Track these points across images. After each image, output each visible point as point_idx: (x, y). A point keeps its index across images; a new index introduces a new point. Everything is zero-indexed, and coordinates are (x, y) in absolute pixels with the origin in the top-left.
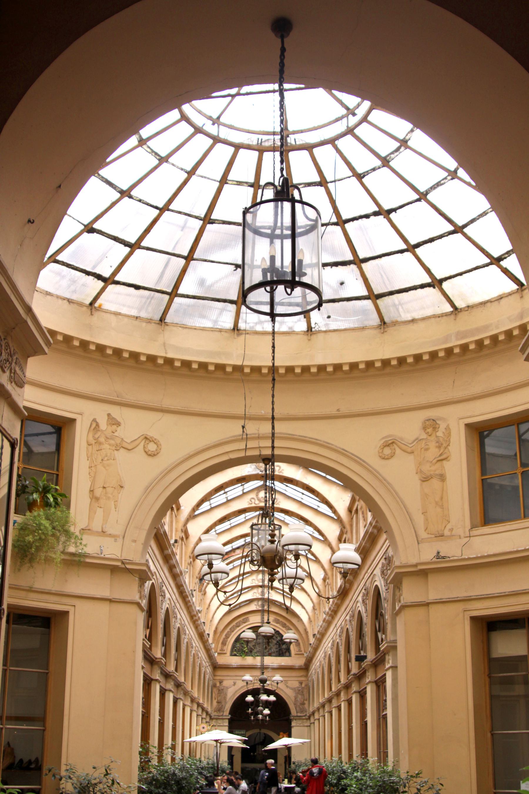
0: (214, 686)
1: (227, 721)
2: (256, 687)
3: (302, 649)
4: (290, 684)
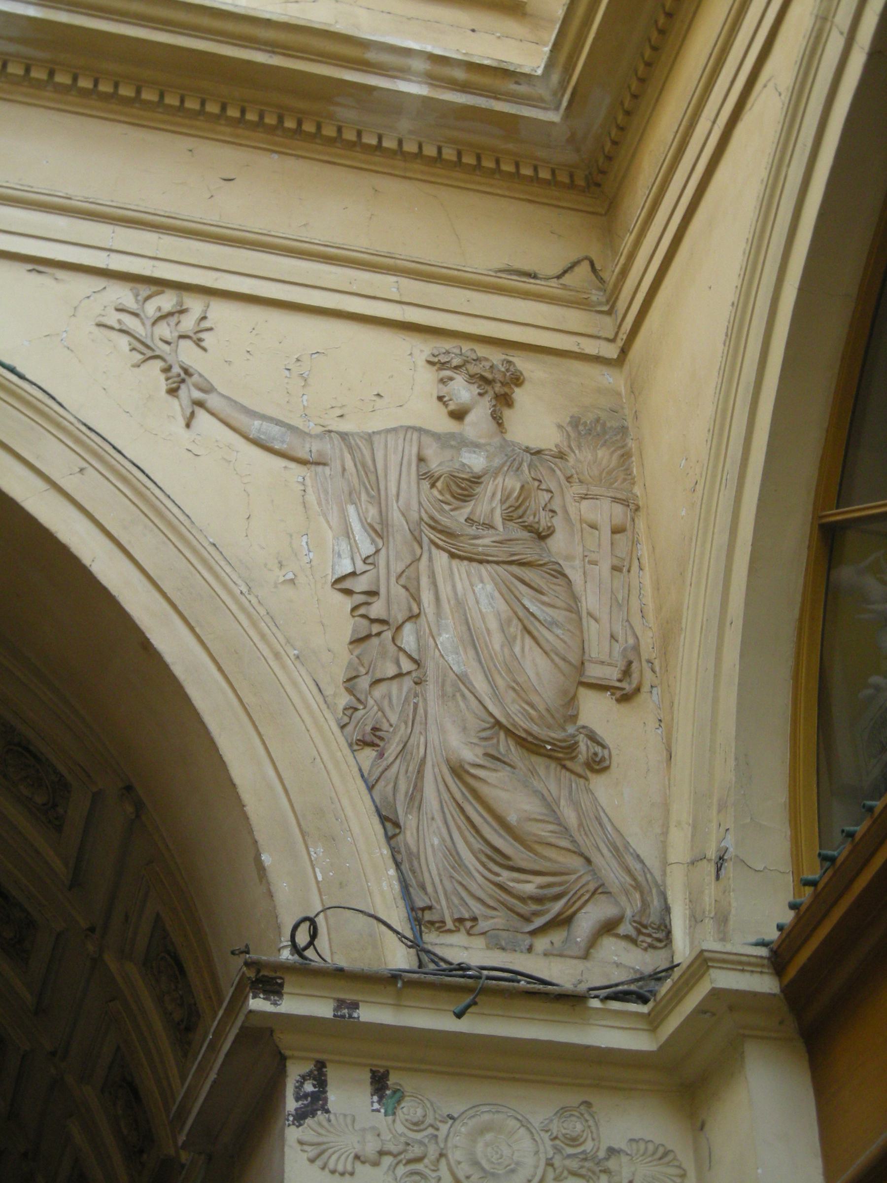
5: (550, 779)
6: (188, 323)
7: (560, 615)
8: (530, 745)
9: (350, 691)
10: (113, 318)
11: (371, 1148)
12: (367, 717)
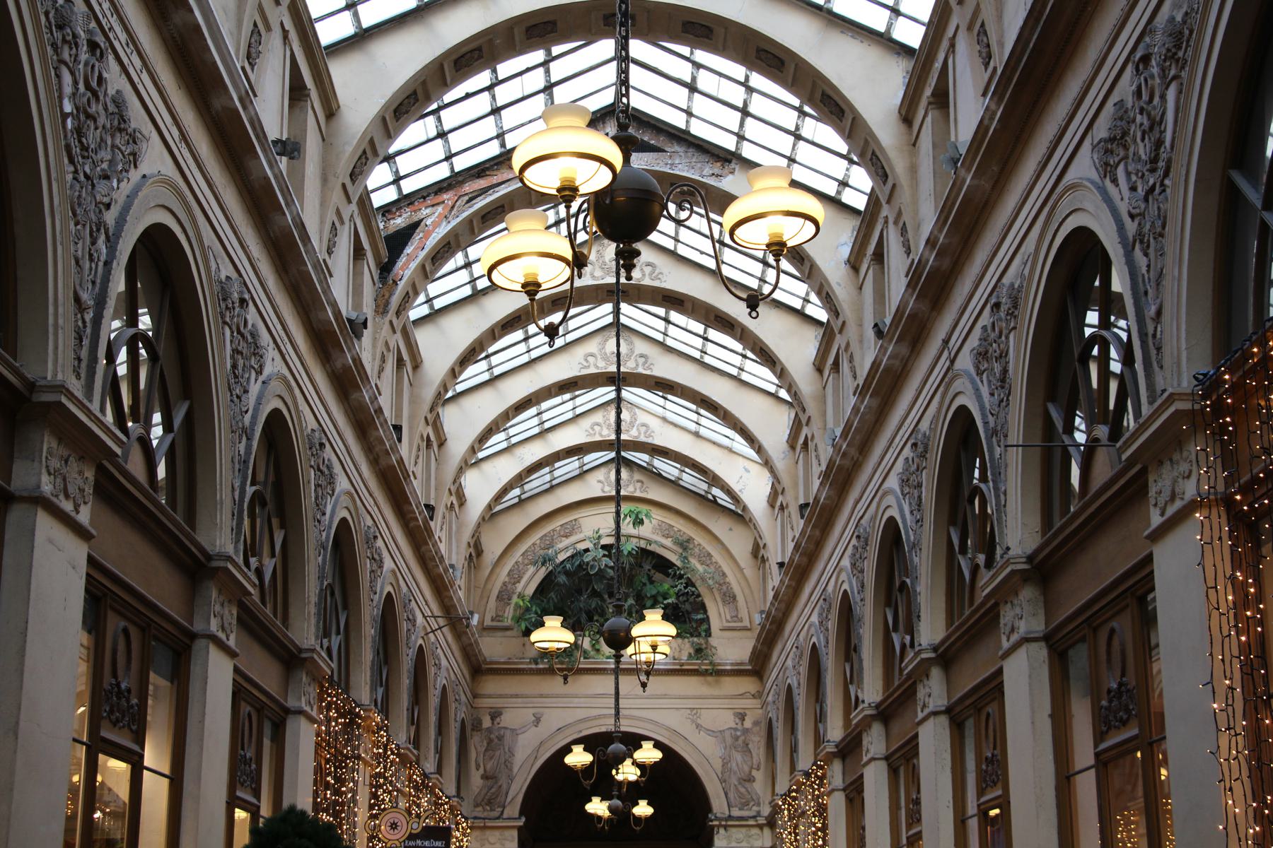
0: (477, 726)
1: (515, 833)
2: (603, 729)
3: (744, 613)
4: (707, 719)
5: (747, 785)
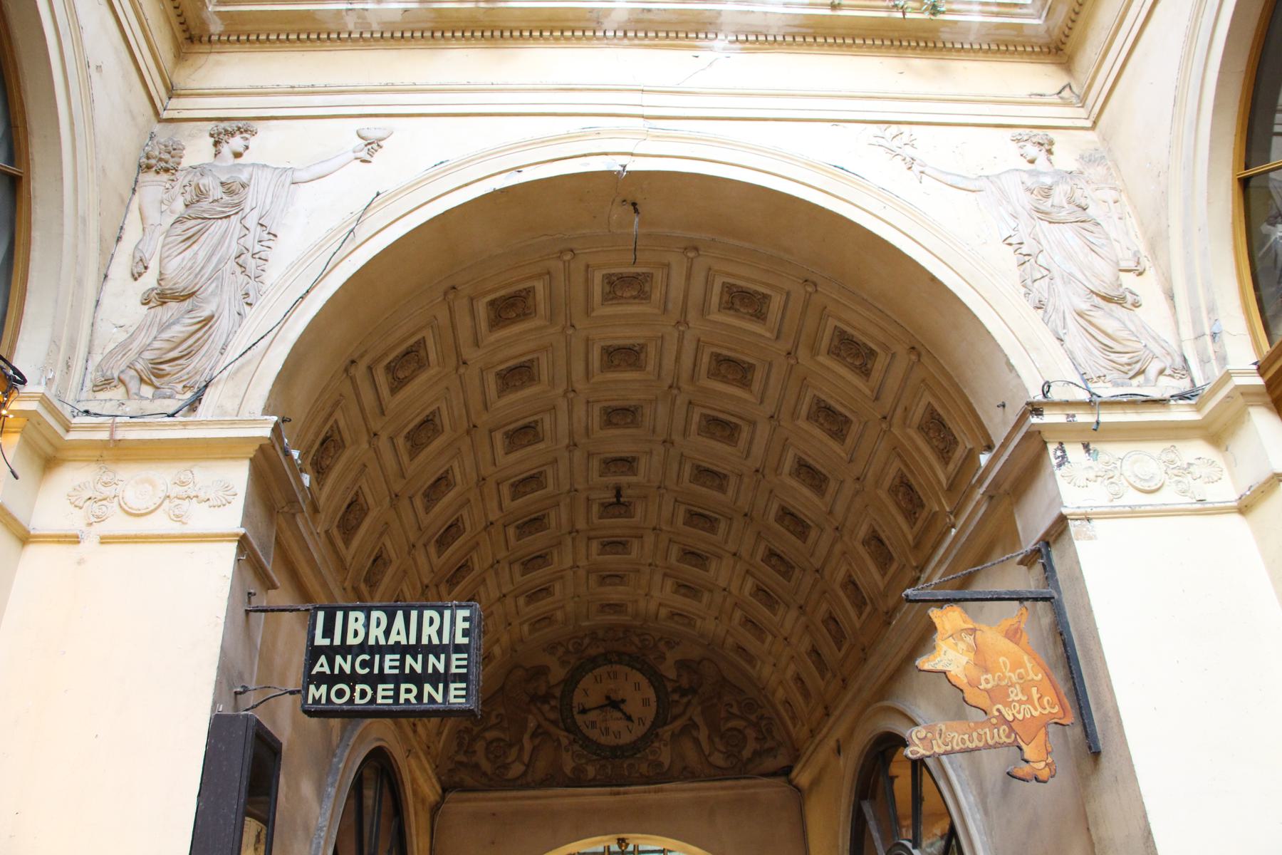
1: (238, 476)
6: (905, 138)
7: (1104, 241)
8: (1108, 299)
9: (1024, 286)
10: (874, 141)
11: (1091, 475)
12: (1035, 296)
